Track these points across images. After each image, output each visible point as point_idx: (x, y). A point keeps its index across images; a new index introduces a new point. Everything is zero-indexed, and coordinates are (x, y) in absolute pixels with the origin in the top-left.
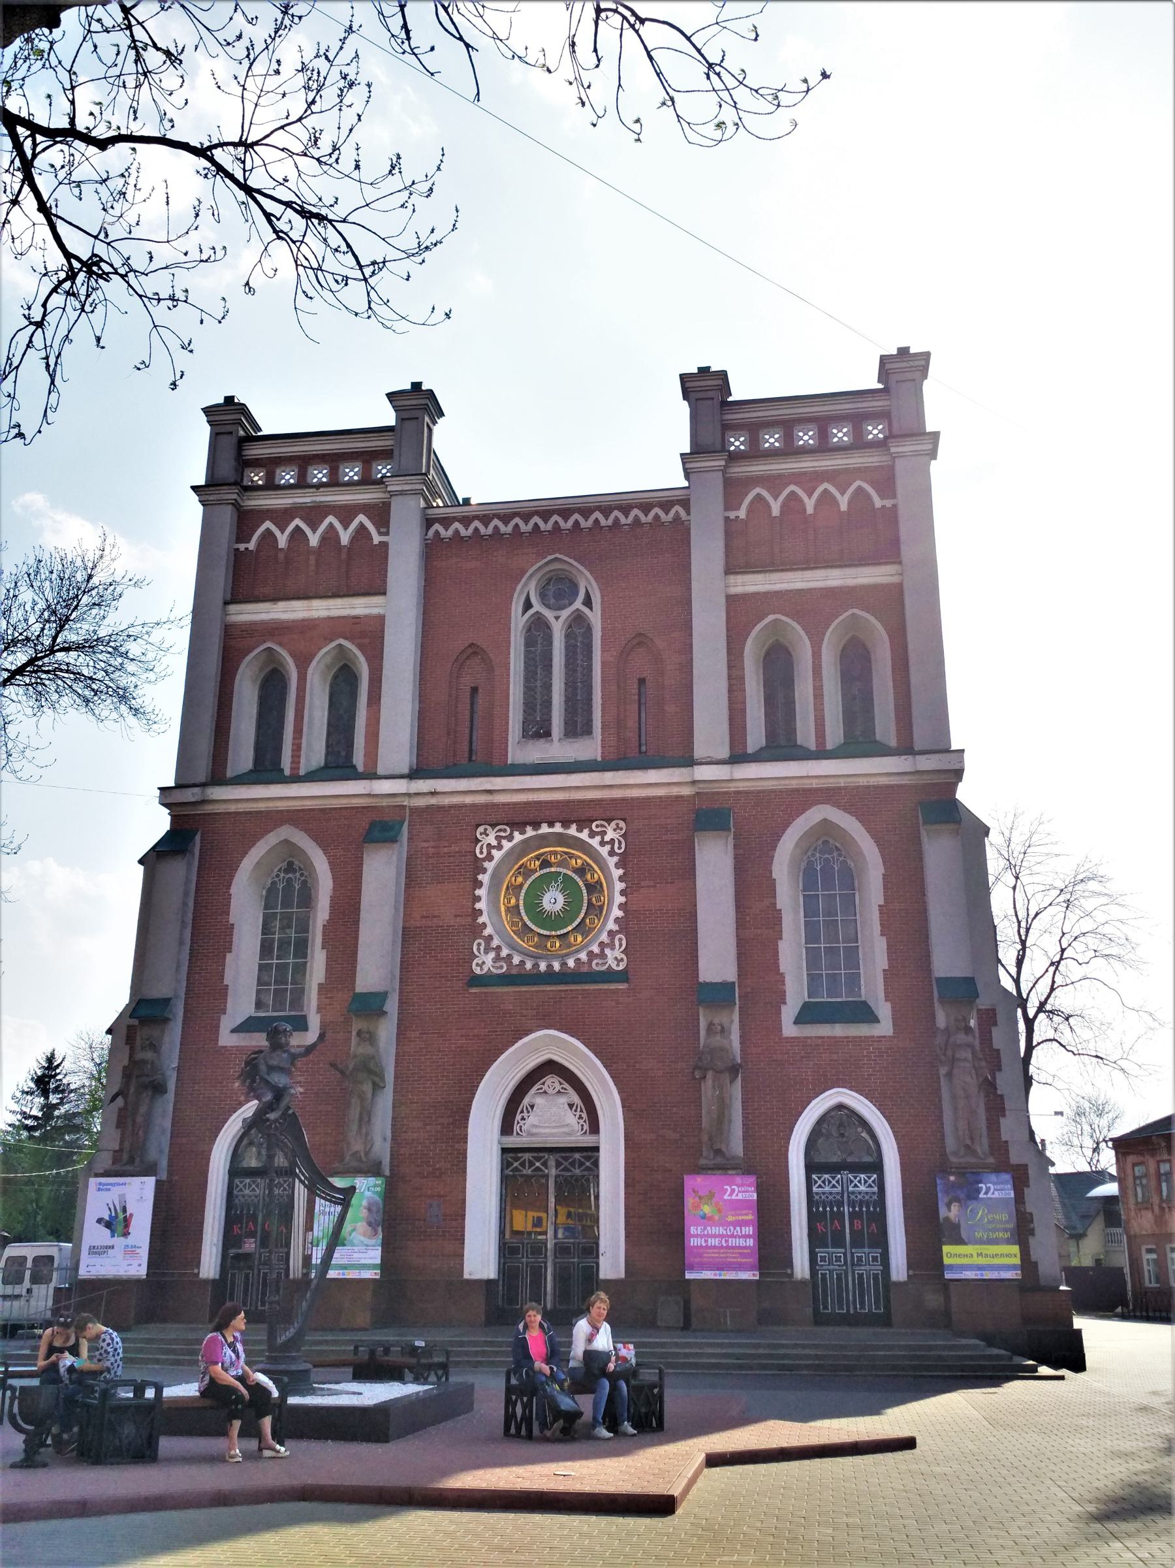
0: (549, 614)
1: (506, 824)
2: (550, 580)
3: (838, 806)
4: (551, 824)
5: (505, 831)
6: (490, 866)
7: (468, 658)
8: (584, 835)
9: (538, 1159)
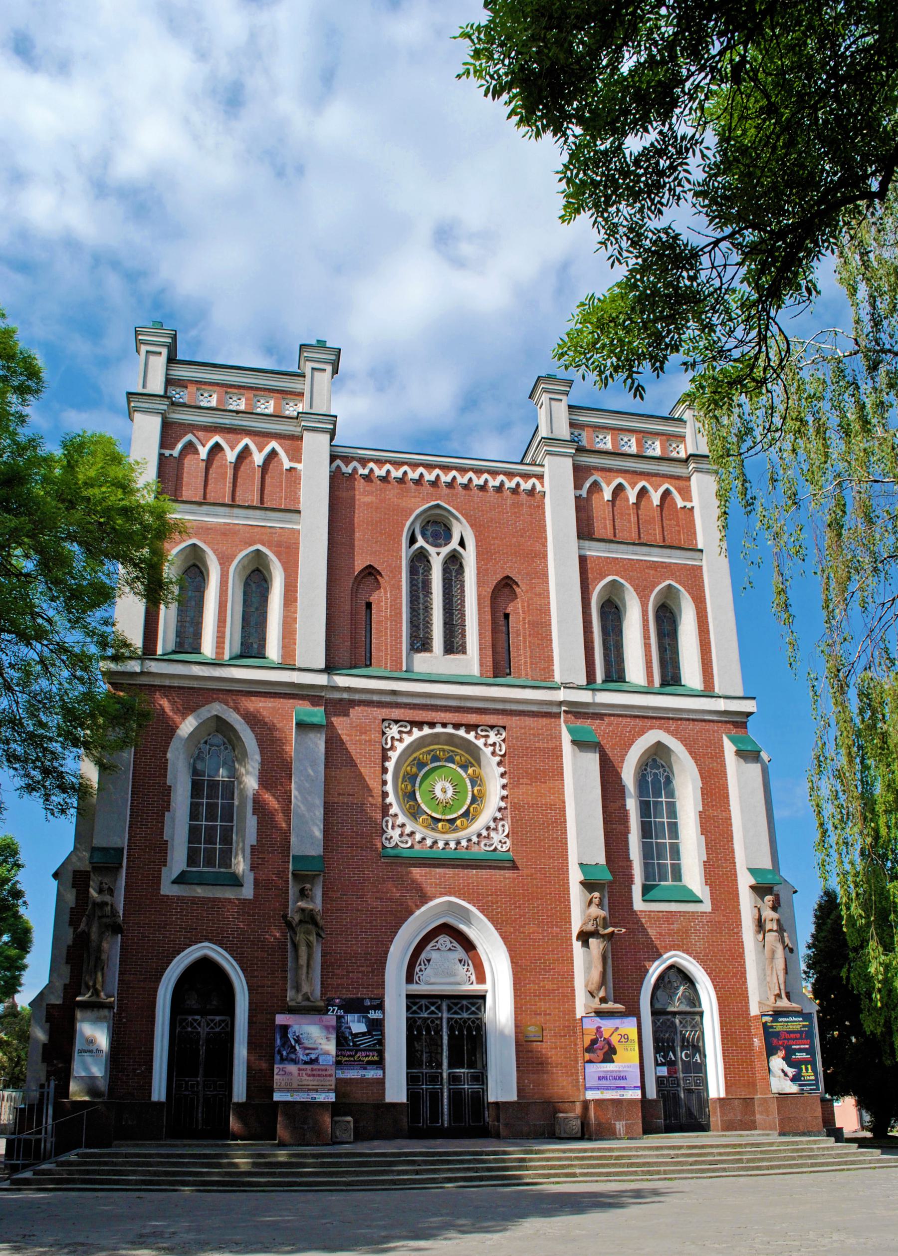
0: (431, 550)
1: (407, 721)
2: (428, 522)
3: (668, 731)
5: (406, 727)
6: (394, 756)
7: (363, 578)
8: (471, 736)
9: (433, 1004)
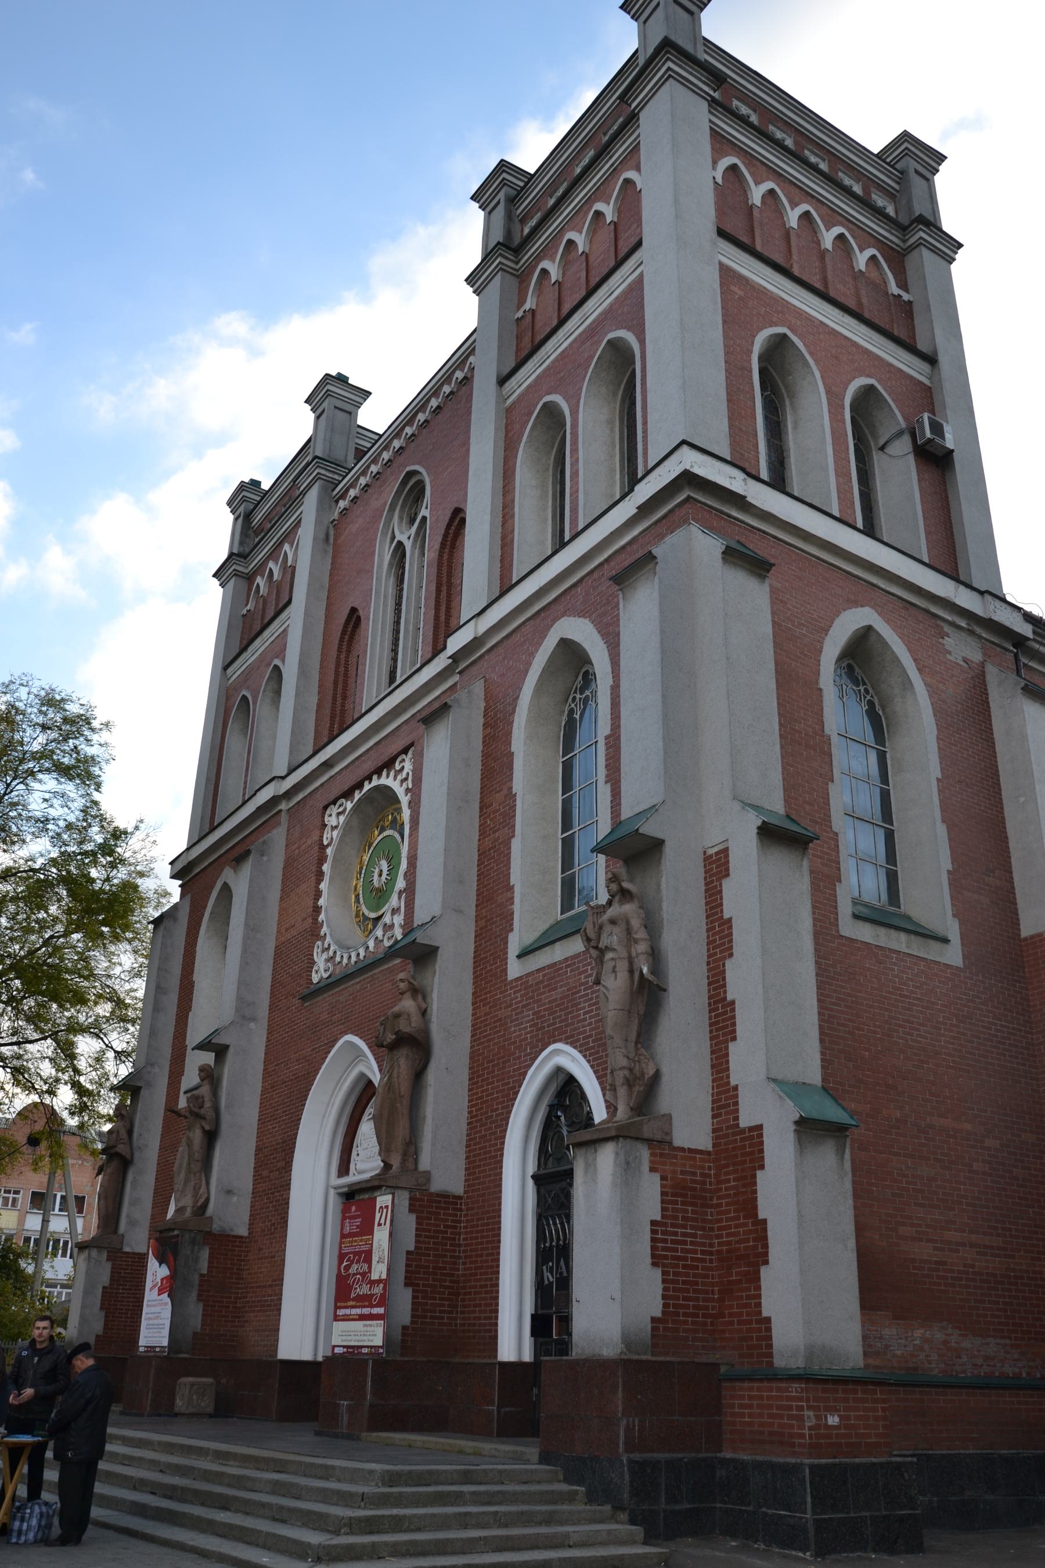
4: (370, 779)
